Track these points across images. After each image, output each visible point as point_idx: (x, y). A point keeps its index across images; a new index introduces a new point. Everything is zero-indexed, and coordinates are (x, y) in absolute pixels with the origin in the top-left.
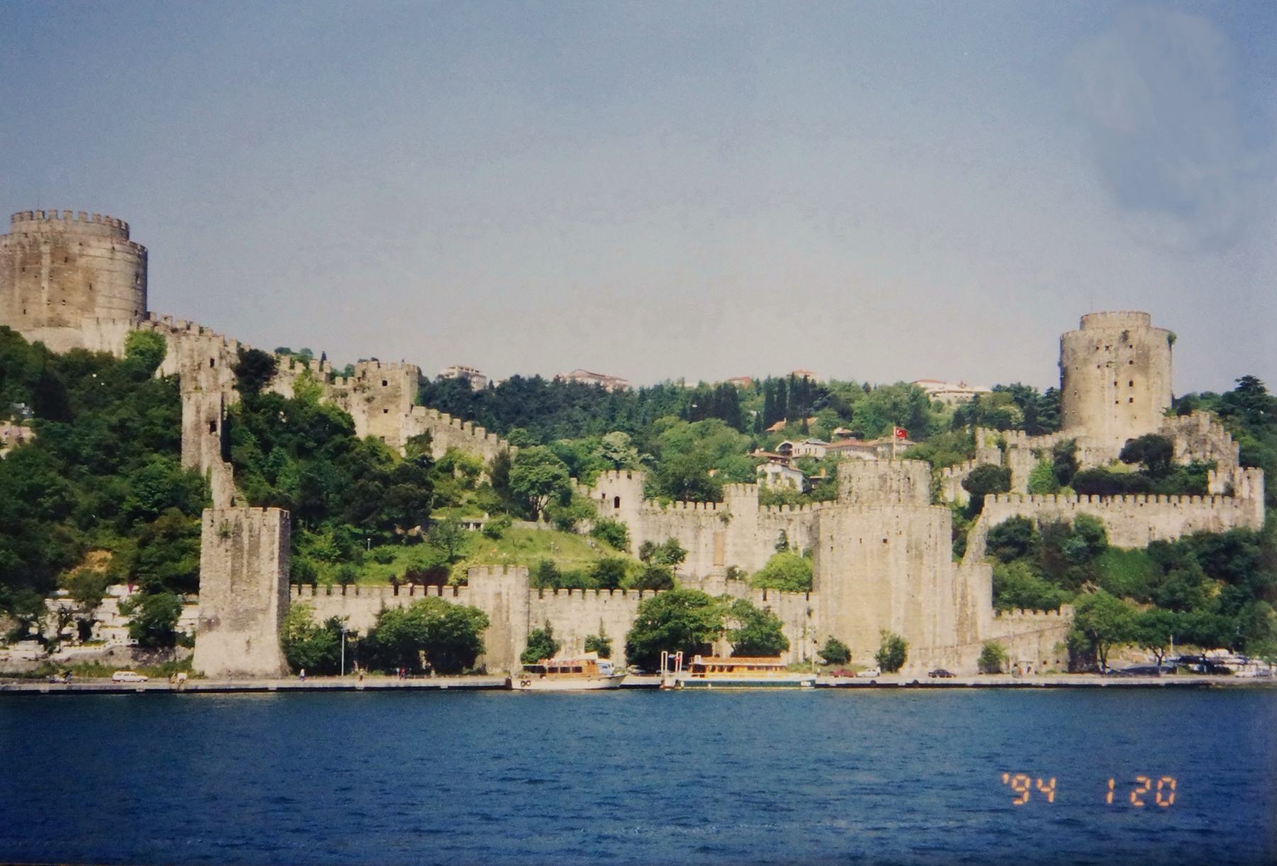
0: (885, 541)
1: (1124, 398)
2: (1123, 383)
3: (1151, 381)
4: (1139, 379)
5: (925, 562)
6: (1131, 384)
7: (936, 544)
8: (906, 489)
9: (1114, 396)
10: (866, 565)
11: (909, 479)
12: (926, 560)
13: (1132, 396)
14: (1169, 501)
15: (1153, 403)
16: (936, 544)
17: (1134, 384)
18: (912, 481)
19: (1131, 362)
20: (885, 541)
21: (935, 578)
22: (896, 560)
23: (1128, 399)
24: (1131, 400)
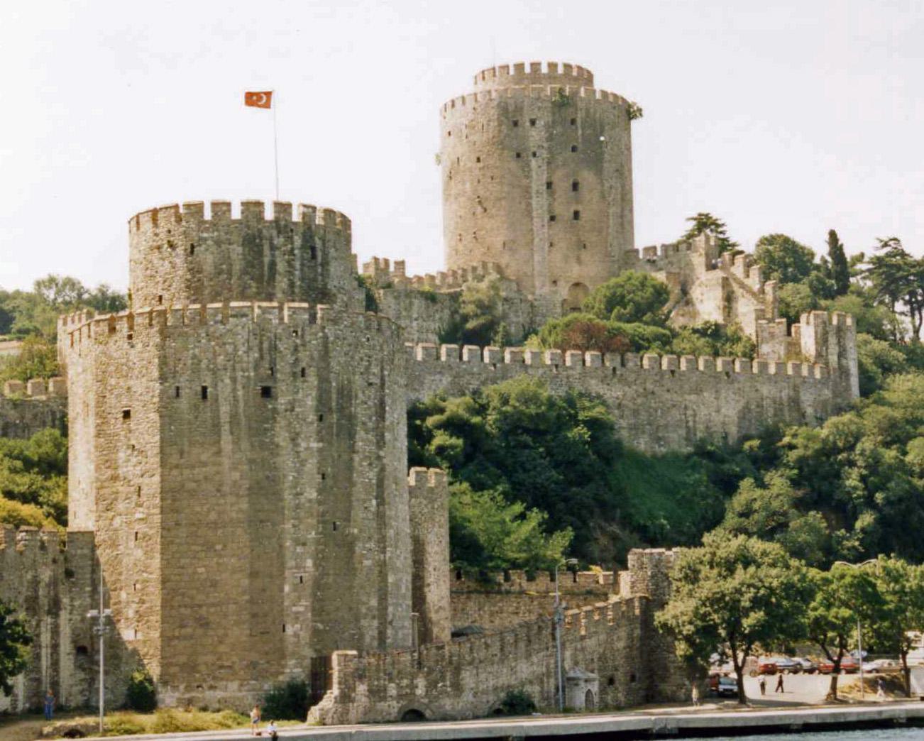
0: (266, 392)
1: (564, 212)
2: (562, 186)
4: (587, 177)
6: (575, 186)
10: (219, 453)
11: (313, 249)
13: (580, 208)
17: (584, 187)
18: (319, 259)
22: (294, 439)
23: (571, 215)
24: (576, 215)
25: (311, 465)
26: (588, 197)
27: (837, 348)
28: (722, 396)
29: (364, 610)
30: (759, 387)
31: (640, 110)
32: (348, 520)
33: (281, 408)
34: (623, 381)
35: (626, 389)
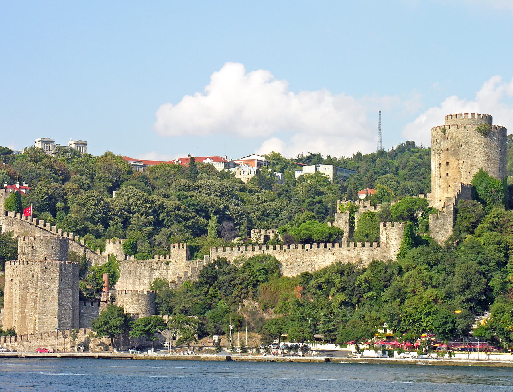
0: (12, 280)
1: (444, 175)
3: (461, 162)
5: (30, 291)
6: (447, 163)
7: (37, 281)
8: (31, 252)
9: (439, 173)
11: (33, 246)
12: (30, 290)
13: (448, 172)
14: (326, 246)
15: (462, 176)
16: (37, 281)
18: (34, 247)
19: (447, 149)
20: (12, 280)
21: (36, 299)
24: (447, 174)
25: (18, 296)
26: (452, 167)
27: (386, 236)
28: (327, 257)
29: (29, 328)
30: (342, 252)
31: (335, 157)
32: (25, 308)
33: (14, 284)
34: (289, 254)
35: (289, 256)
